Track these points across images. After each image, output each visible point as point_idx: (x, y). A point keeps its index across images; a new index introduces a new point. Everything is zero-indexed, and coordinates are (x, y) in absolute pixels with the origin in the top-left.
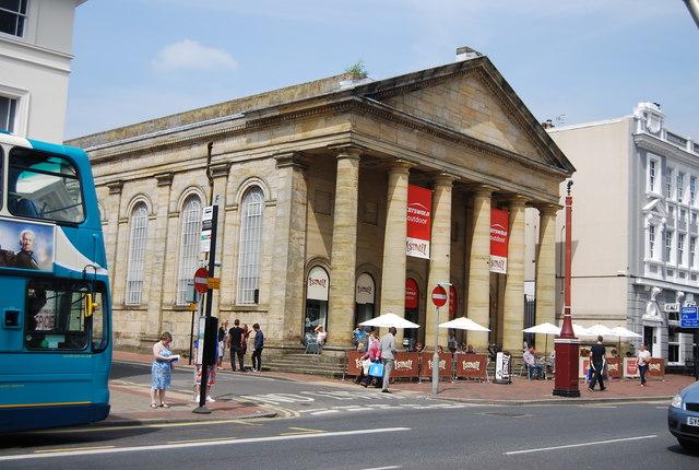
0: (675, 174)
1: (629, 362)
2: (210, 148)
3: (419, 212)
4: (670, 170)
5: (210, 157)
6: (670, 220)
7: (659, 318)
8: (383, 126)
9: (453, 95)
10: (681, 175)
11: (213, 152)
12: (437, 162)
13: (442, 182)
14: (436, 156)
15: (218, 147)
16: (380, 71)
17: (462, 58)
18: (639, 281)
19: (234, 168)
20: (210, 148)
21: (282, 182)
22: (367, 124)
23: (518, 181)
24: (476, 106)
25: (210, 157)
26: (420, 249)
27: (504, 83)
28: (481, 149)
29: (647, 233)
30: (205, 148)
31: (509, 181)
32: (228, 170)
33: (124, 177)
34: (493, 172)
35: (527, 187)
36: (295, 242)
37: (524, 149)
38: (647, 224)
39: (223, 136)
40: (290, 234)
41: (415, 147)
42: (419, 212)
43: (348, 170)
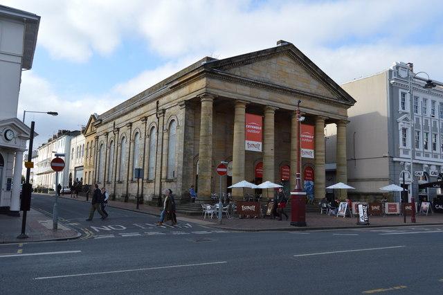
0: (420, 100)
1: (389, 206)
2: (158, 103)
3: (255, 127)
4: (417, 98)
5: (157, 107)
6: (417, 125)
8: (227, 84)
9: (273, 66)
10: (425, 100)
11: (160, 105)
13: (268, 111)
14: (263, 97)
15: (162, 101)
16: (221, 55)
17: (280, 45)
18: (395, 159)
19: (167, 111)
20: (158, 103)
21: (180, 114)
22: (216, 83)
24: (288, 70)
25: (157, 107)
26: (255, 146)
28: (291, 92)
29: (401, 132)
30: (154, 104)
32: (164, 113)
33: (132, 121)
36: (188, 147)
37: (324, 92)
39: (161, 96)
40: (185, 142)
41: (248, 93)
42: (255, 127)
43: (206, 105)
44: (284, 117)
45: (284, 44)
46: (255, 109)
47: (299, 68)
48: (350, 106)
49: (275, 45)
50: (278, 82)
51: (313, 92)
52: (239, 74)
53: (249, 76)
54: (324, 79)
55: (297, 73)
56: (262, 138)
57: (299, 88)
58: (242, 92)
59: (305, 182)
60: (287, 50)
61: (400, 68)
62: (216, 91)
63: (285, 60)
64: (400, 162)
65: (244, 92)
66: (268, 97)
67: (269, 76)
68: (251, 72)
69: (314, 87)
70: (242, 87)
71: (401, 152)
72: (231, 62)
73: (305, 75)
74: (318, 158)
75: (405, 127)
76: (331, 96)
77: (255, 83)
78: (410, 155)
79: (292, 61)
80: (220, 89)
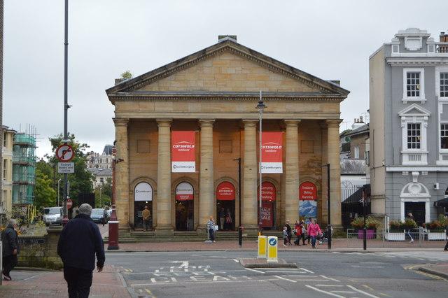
3: (185, 146)
7: (427, 194)
9: (206, 70)
12: (193, 114)
14: (192, 111)
22: (128, 105)
23: (285, 110)
26: (187, 167)
27: (251, 51)
29: (405, 131)
31: (272, 112)
34: (249, 111)
35: (295, 113)
37: (291, 87)
38: (405, 125)
41: (171, 109)
44: (228, 129)
45: (224, 39)
46: (182, 125)
47: (248, 64)
48: (342, 99)
49: (216, 41)
50: (214, 88)
51: (274, 89)
52: (157, 90)
53: (171, 89)
54: (291, 72)
55: (245, 72)
56: (196, 157)
57: (248, 90)
58: (161, 109)
59: (301, 203)
60: (227, 46)
61: (406, 38)
62: (128, 114)
63: (226, 58)
64: (401, 172)
65: (165, 109)
66: (200, 110)
67: (201, 84)
68: (173, 85)
69: (276, 84)
70: (163, 104)
71: (406, 161)
72: (144, 80)
73: (260, 72)
74: (287, 172)
75: (415, 121)
76: (310, 90)
77: (175, 97)
78: (424, 161)
79: (238, 58)
80: (132, 111)
